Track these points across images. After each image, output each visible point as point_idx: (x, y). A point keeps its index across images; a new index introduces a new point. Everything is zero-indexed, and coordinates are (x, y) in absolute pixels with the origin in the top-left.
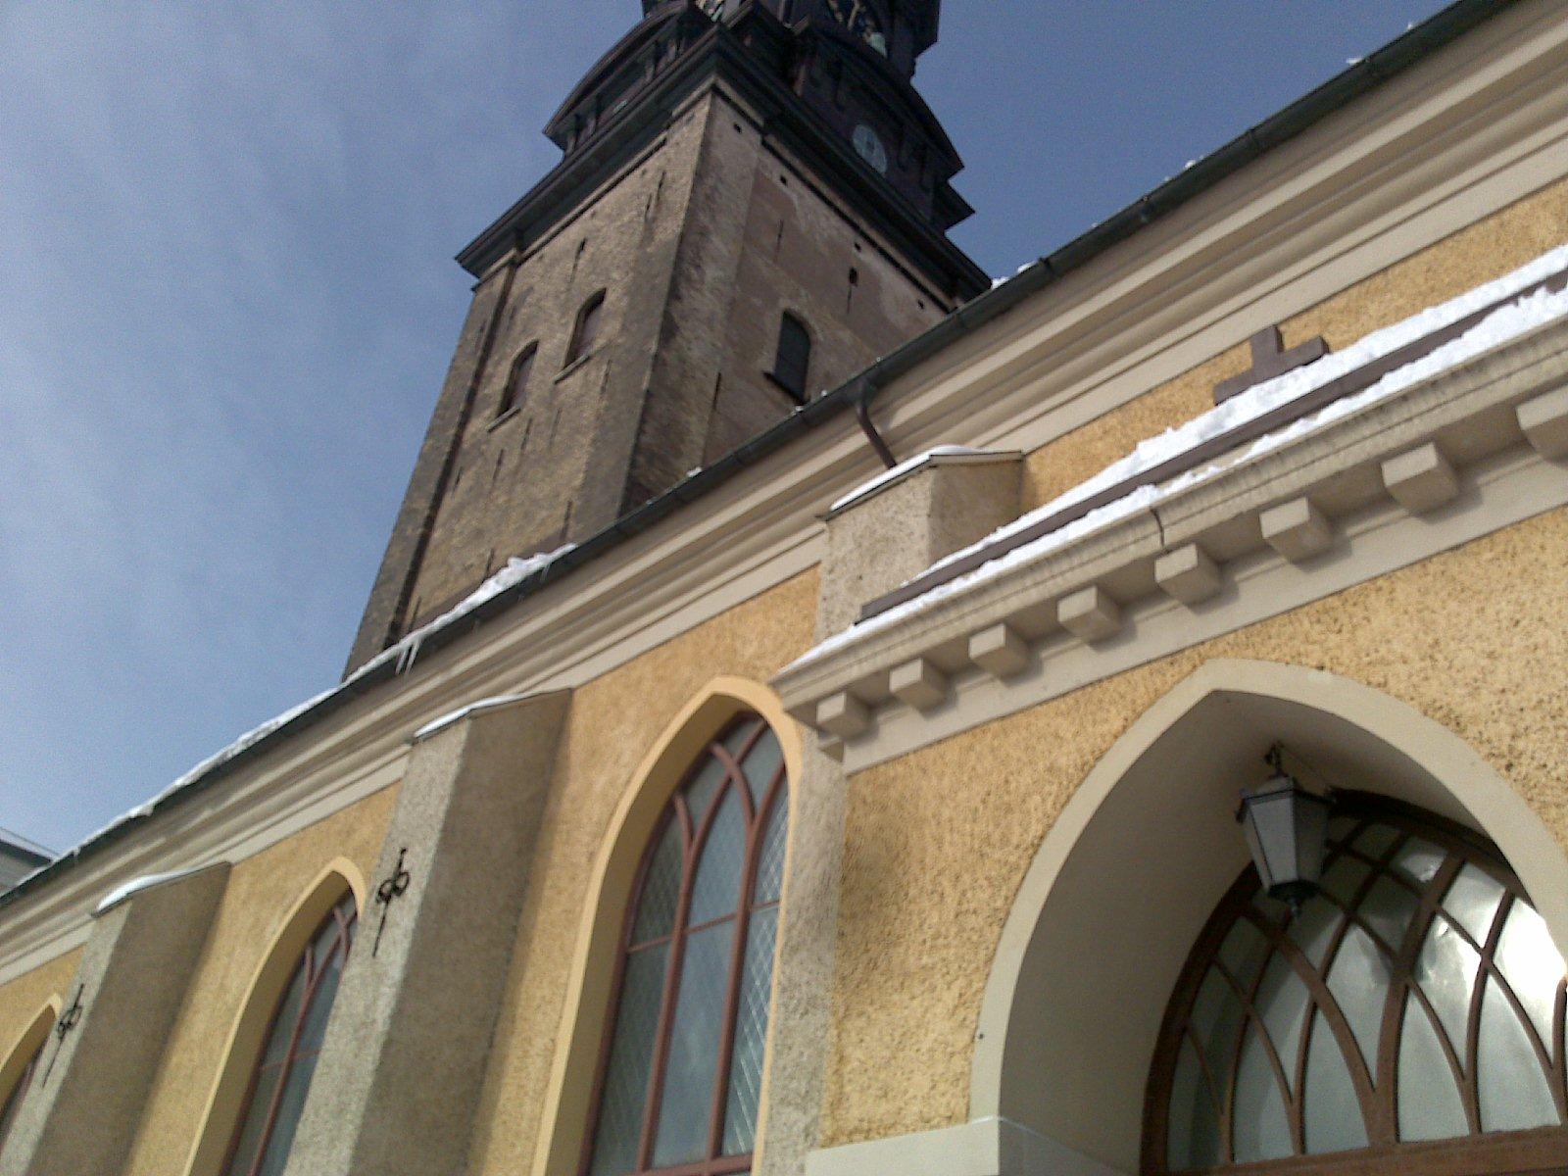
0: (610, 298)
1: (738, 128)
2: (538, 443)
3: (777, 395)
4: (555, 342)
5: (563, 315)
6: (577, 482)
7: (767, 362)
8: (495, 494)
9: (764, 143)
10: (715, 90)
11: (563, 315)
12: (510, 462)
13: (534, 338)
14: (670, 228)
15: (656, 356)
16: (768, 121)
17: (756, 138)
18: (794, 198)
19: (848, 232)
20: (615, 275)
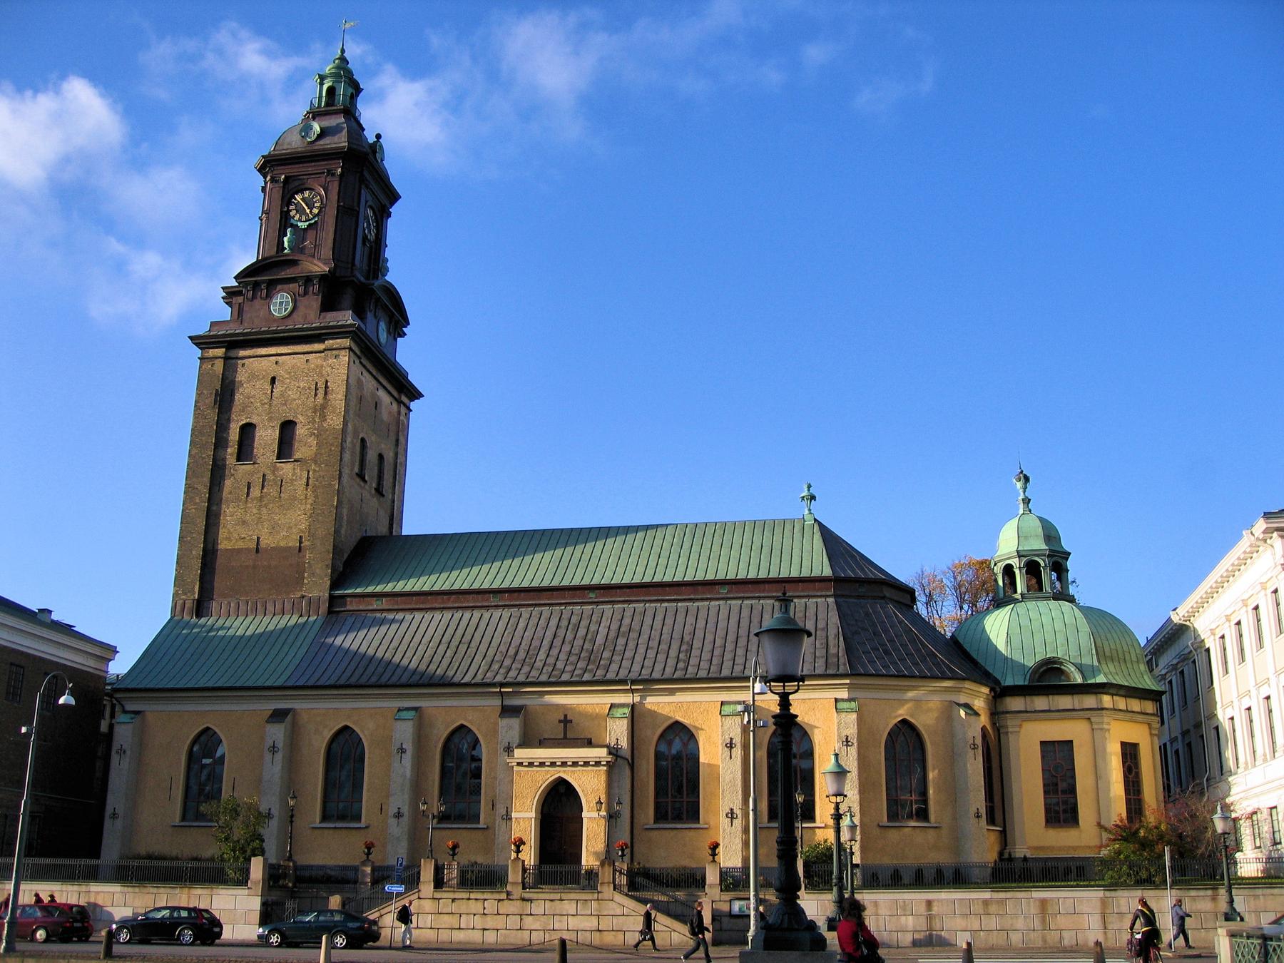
0: (300, 431)
1: (354, 362)
2: (271, 490)
3: (358, 480)
4: (267, 437)
5: (270, 419)
6: (302, 526)
7: (356, 470)
8: (250, 505)
9: (360, 362)
10: (350, 349)
11: (270, 419)
12: (255, 492)
13: (253, 421)
14: (335, 421)
15: (338, 490)
16: (361, 351)
17: (357, 362)
18: (363, 379)
19: (374, 382)
20: (300, 419)
